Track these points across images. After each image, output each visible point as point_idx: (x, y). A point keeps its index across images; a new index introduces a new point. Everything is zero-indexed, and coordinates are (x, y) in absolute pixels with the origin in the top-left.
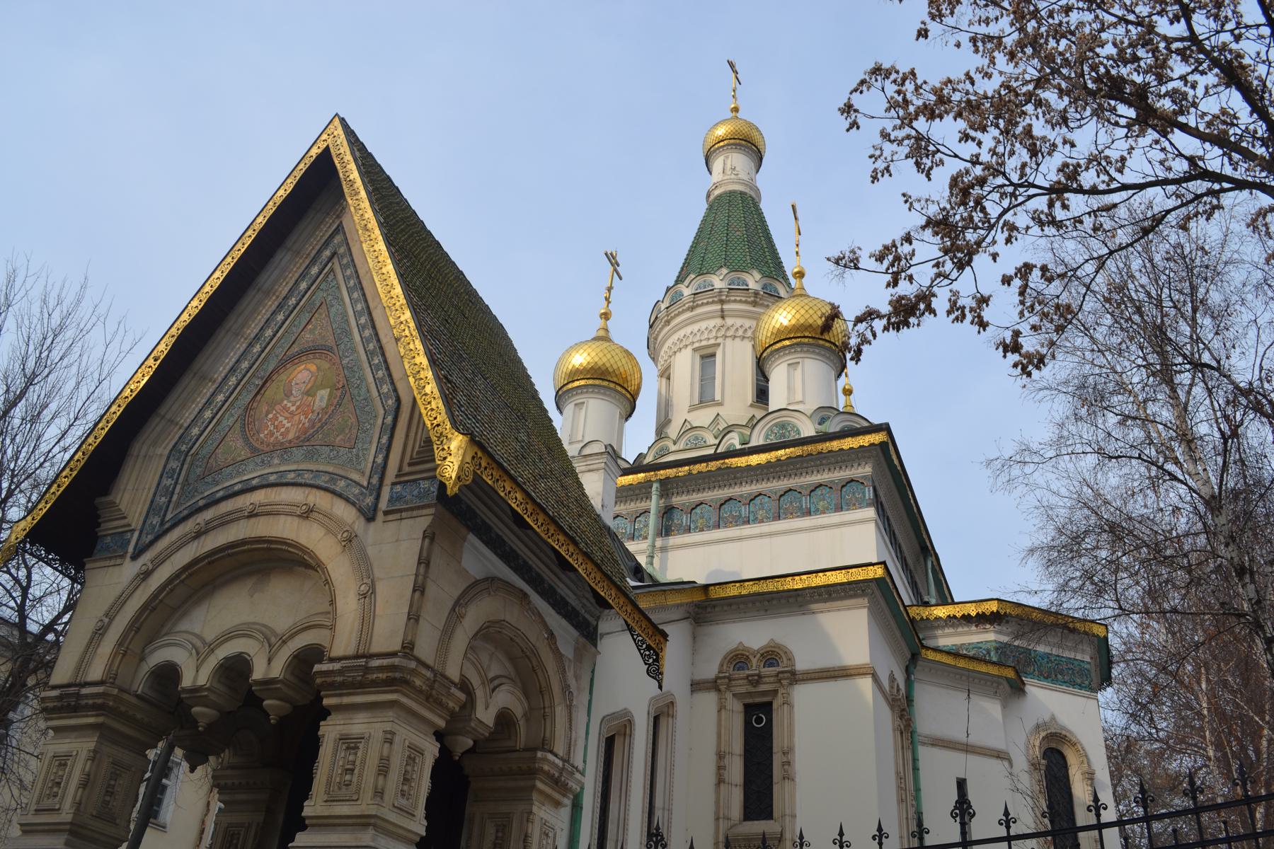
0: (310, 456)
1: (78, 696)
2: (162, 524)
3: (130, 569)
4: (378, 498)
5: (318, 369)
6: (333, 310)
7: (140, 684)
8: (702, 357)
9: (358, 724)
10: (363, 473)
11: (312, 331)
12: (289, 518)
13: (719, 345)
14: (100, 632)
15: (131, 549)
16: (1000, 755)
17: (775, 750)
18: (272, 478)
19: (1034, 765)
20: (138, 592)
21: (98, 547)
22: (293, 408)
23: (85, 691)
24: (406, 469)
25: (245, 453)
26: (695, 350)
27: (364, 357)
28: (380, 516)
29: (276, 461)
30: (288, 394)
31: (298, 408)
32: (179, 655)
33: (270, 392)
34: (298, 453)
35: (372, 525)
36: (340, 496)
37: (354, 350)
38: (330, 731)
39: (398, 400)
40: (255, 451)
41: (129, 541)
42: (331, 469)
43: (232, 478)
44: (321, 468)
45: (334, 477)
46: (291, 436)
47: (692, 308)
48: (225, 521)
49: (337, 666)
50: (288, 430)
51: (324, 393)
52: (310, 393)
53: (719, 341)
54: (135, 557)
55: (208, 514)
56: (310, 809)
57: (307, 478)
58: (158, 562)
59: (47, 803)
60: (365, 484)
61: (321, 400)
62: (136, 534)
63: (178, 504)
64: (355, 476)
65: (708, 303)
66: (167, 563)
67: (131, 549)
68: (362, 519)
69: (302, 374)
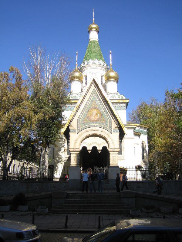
7: (81, 149)
9: (114, 155)
11: (94, 105)
14: (76, 142)
17: (122, 147)
18: (95, 126)
21: (70, 131)
23: (76, 149)
25: (89, 121)
28: (112, 133)
30: (93, 114)
33: (90, 112)
38: (111, 155)
40: (90, 121)
46: (95, 120)
48: (91, 130)
50: (94, 119)
51: (99, 115)
57: (101, 127)
58: (82, 134)
63: (81, 127)
69: (94, 111)
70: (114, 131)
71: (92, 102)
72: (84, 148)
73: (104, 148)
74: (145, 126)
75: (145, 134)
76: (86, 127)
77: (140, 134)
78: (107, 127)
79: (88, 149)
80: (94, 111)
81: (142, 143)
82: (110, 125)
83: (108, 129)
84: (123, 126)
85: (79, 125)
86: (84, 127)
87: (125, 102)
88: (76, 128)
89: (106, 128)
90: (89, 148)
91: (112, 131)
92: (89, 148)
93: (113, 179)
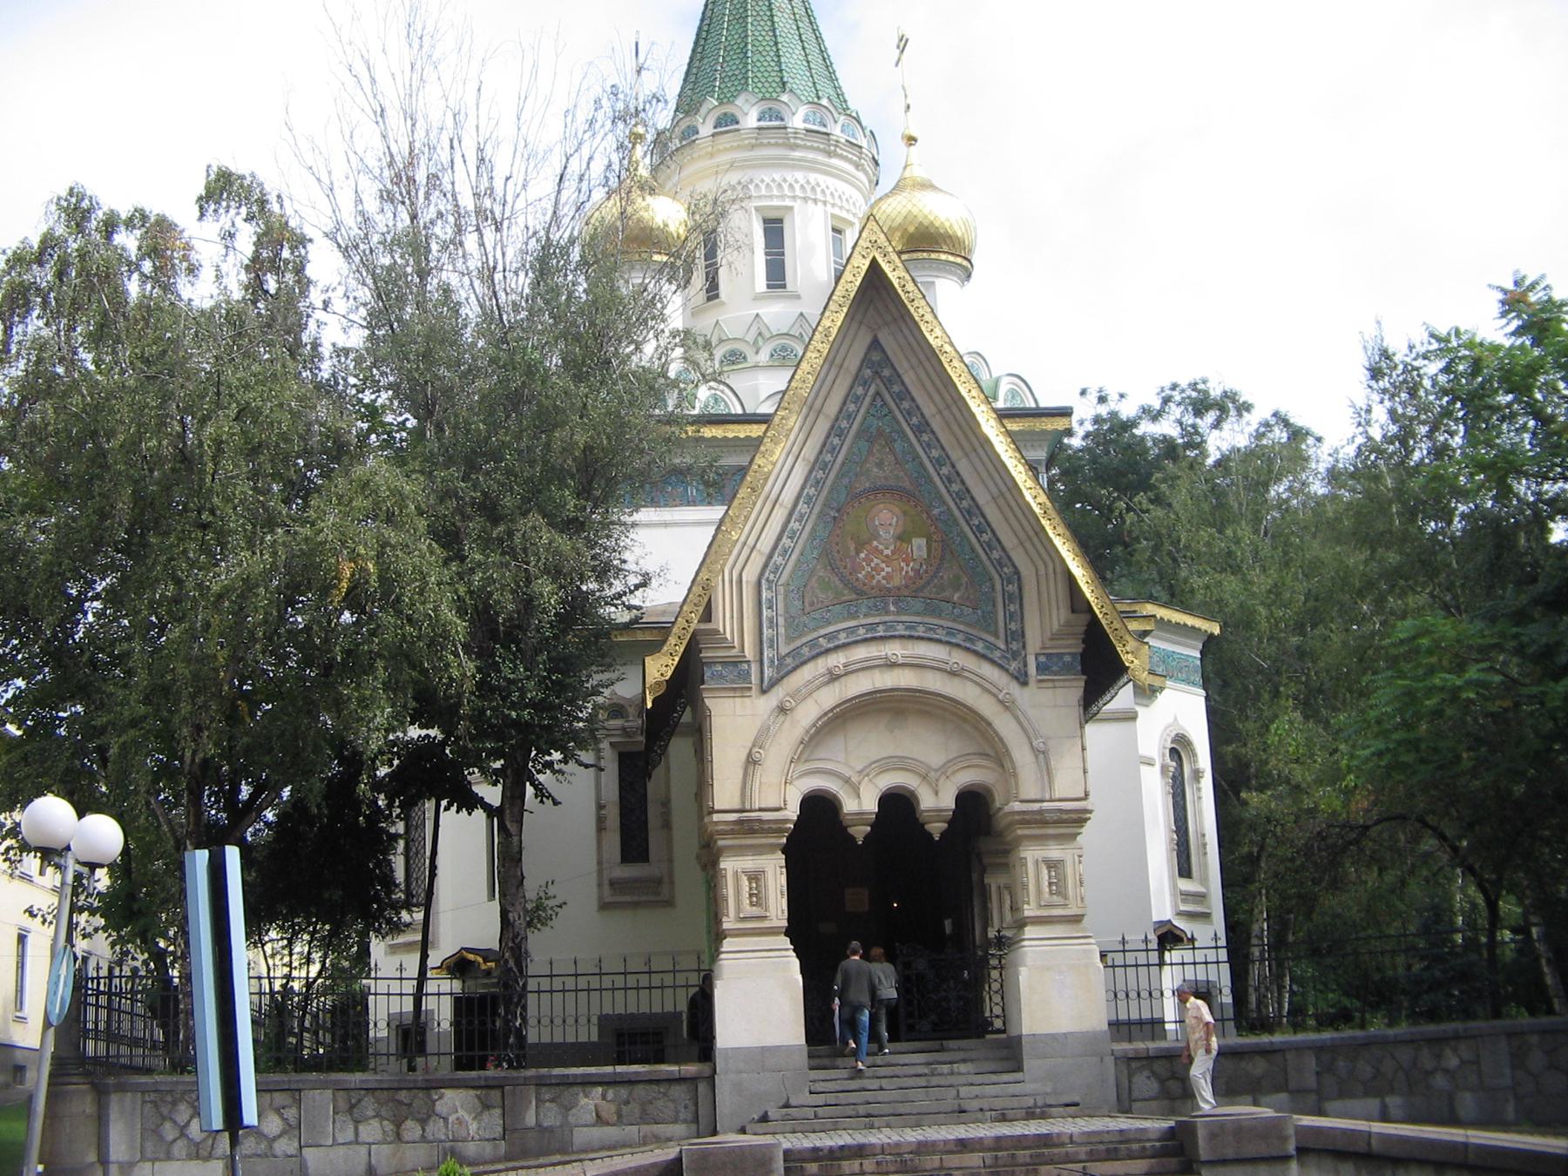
0: (931, 610)
1: (760, 821)
2: (781, 659)
3: (763, 705)
4: (1025, 665)
5: (905, 513)
6: (898, 446)
8: (766, 221)
10: (996, 635)
11: (880, 465)
12: (938, 675)
13: (791, 208)
14: (751, 762)
15: (754, 678)
16: (1150, 763)
19: (1164, 769)
20: (787, 725)
21: (707, 674)
22: (887, 552)
24: (1049, 644)
26: (757, 209)
27: (957, 513)
29: (892, 608)
30: (876, 537)
31: (893, 553)
32: (832, 785)
34: (918, 605)
35: (1027, 691)
36: (984, 657)
37: (944, 503)
39: (1017, 572)
40: (861, 594)
41: (748, 673)
42: (962, 627)
43: (845, 619)
44: (950, 624)
45: (969, 638)
46: (897, 581)
47: (753, 147)
48: (867, 667)
49: (1036, 806)
50: (888, 577)
52: (903, 538)
53: (788, 203)
54: (764, 692)
55: (837, 660)
56: (1029, 911)
57: (941, 634)
58: (800, 696)
59: (756, 911)
60: (1003, 647)
61: (919, 547)
62: (754, 668)
63: (789, 639)
64: (991, 639)
65: (776, 145)
66: (810, 701)
67: (754, 678)
68: (1014, 688)
70: (1041, 669)
71: (863, 444)
72: (819, 807)
73: (973, 803)
74: (1190, 621)
75: (1188, 682)
76: (830, 637)
77: (1157, 682)
78: (991, 639)
79: (849, 805)
80: (887, 518)
81: (1174, 753)
82: (1011, 617)
83: (996, 655)
84: (1116, 625)
85: (772, 624)
86: (813, 643)
87: (1044, 432)
88: (749, 653)
89: (979, 647)
90: (860, 802)
91: (1032, 669)
92: (860, 802)
93: (1053, 1037)
